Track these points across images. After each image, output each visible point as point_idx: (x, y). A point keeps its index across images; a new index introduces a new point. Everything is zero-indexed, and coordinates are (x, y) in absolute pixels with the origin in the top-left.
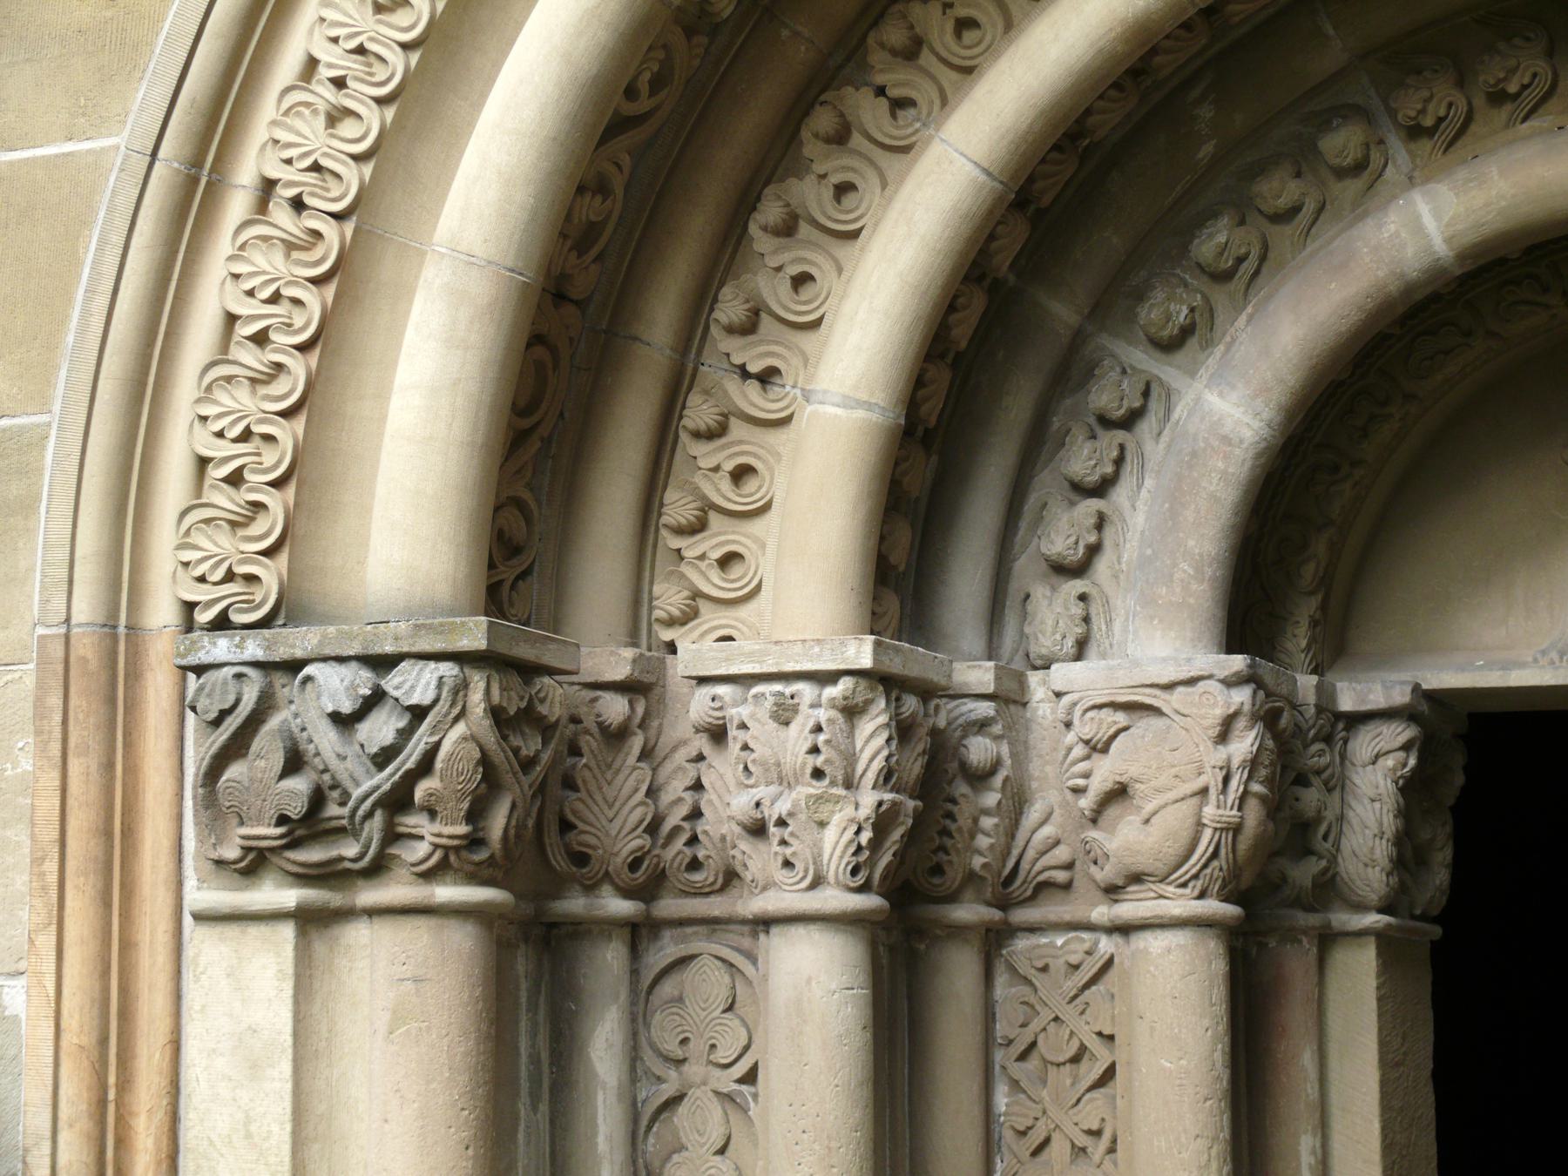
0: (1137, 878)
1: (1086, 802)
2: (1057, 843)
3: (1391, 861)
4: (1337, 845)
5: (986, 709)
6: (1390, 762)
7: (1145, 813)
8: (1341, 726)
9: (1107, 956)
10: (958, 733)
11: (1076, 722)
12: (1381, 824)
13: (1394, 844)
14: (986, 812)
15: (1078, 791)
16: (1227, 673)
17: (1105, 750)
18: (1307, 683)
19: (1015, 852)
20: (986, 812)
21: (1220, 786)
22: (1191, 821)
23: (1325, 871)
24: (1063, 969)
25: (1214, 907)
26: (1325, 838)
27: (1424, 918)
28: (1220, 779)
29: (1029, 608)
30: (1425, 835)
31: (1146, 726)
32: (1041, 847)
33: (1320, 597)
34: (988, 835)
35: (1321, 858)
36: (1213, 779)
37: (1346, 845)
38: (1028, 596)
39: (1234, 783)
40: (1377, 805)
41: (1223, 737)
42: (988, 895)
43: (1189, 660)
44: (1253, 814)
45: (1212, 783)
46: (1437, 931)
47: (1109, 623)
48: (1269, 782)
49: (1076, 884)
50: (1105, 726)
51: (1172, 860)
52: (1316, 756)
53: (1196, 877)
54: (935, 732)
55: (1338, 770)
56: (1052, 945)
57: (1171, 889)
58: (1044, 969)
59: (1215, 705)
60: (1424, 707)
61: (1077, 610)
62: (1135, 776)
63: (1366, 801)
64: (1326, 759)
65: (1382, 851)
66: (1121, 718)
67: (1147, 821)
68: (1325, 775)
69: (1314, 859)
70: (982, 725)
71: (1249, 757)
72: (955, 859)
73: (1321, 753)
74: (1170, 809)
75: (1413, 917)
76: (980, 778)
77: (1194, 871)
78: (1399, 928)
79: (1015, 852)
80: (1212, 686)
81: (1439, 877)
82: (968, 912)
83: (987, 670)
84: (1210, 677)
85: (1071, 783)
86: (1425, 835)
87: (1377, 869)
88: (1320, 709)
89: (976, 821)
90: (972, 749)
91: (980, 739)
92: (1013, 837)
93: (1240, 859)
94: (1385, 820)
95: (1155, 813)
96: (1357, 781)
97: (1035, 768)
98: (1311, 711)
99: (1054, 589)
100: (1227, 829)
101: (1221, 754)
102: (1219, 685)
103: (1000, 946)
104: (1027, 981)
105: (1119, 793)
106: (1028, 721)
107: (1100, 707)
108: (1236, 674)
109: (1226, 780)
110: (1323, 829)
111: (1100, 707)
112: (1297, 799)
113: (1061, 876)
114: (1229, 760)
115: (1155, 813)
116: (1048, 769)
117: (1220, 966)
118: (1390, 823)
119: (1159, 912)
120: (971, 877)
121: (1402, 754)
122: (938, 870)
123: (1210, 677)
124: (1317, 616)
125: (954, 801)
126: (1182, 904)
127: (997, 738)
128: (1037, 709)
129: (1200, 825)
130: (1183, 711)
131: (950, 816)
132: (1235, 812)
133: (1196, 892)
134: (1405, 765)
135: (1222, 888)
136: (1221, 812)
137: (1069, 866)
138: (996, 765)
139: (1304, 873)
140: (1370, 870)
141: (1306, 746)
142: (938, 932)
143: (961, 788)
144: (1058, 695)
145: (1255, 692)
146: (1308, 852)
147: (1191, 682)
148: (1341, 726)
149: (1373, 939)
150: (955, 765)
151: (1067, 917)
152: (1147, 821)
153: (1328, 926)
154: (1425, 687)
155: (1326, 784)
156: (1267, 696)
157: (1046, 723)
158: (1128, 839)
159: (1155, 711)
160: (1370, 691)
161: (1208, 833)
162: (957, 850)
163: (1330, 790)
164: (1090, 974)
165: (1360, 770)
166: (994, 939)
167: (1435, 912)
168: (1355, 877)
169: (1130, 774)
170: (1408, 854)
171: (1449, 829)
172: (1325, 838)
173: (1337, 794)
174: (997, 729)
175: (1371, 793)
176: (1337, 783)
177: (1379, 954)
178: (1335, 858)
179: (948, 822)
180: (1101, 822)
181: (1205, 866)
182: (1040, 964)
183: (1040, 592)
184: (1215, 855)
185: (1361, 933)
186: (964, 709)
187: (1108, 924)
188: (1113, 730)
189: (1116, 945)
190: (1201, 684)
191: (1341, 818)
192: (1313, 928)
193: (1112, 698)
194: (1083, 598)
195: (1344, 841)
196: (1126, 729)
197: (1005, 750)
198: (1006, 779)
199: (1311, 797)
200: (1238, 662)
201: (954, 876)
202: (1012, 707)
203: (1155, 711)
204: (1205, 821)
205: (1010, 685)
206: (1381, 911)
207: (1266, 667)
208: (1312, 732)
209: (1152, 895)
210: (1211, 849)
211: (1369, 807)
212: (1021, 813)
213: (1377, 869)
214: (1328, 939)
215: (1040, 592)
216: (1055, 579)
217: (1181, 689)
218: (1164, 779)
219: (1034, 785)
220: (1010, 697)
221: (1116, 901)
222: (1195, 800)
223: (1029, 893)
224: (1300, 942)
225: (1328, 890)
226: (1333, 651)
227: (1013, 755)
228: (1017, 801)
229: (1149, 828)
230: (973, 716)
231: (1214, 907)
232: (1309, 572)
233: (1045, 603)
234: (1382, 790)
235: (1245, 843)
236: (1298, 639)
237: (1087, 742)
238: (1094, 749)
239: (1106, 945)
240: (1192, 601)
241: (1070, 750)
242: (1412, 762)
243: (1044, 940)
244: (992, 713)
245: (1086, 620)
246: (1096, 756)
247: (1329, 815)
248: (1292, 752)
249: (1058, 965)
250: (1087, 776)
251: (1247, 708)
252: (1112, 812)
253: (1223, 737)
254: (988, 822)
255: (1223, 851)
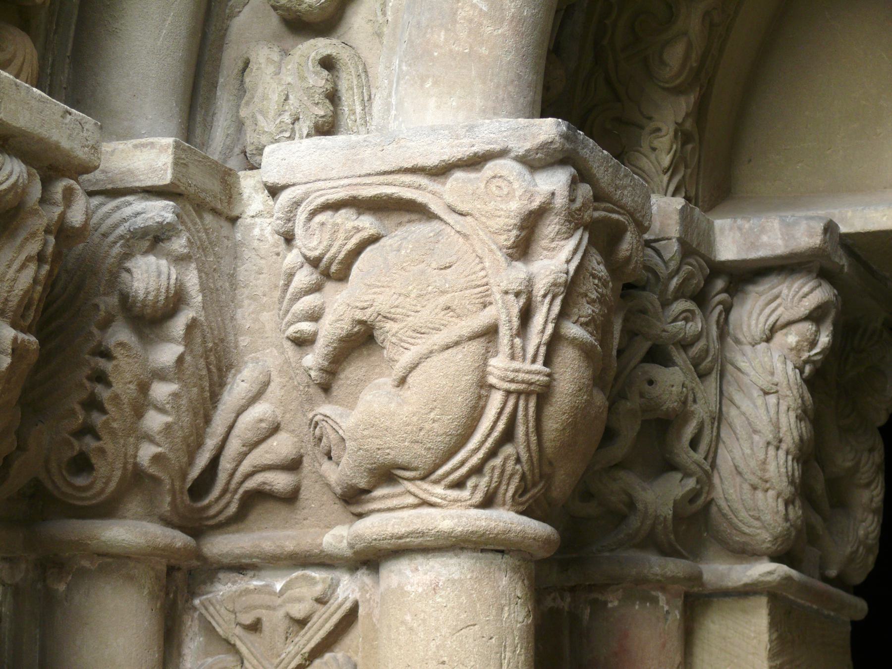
0: (387, 474)
1: (313, 359)
2: (275, 429)
3: (792, 482)
4: (712, 457)
5: (160, 211)
6: (791, 338)
7: (398, 370)
8: (720, 284)
9: (348, 605)
10: (117, 250)
11: (299, 231)
12: (777, 427)
13: (796, 459)
14: (160, 375)
15: (302, 342)
16: (528, 145)
17: (342, 276)
18: (666, 210)
19: (211, 444)
20: (160, 375)
21: (516, 322)
22: (468, 379)
23: (693, 497)
24: (283, 625)
25: (505, 519)
26: (694, 444)
27: (839, 582)
28: (515, 311)
29: (247, 80)
30: (844, 460)
31: (407, 235)
32: (251, 436)
33: (692, 98)
34: (162, 410)
35: (687, 474)
36: (505, 313)
37: (724, 458)
38: (247, 63)
39: (538, 320)
40: (772, 399)
41: (523, 248)
42: (165, 505)
43: (471, 128)
44: (570, 372)
45: (503, 317)
46: (860, 607)
47: (367, 102)
48: (599, 326)
49: (303, 494)
50: (341, 235)
51: (440, 443)
52: (679, 320)
53: (477, 470)
54: (64, 233)
55: (714, 345)
56: (267, 590)
57: (439, 490)
58: (255, 627)
59: (509, 196)
60: (842, 260)
61: (319, 80)
62: (384, 309)
63: (756, 393)
64: (695, 326)
65: (779, 467)
66: (368, 224)
67: (402, 381)
68: (695, 350)
69: (679, 476)
70: (155, 238)
71: (563, 278)
72: (109, 447)
73: (688, 316)
74: (436, 359)
75: (825, 579)
76: (150, 320)
77: (474, 460)
78: (804, 589)
79: (211, 444)
80: (507, 167)
81: (864, 526)
82: (126, 532)
83: (163, 149)
84: (503, 153)
85: (291, 330)
86: (844, 460)
87: (771, 493)
88: (687, 250)
89: (144, 388)
90: (137, 273)
91: (152, 259)
92: (208, 420)
93: (548, 444)
94: (783, 420)
95: (414, 367)
96: (743, 364)
97: (246, 315)
98: (675, 247)
99: (285, 53)
100: (528, 394)
101: (517, 274)
102: (518, 167)
103: (193, 594)
104: (232, 648)
105: (361, 340)
106: (236, 245)
107: (335, 206)
108: (544, 146)
109: (526, 315)
110: (689, 431)
111: (335, 206)
112: (651, 382)
113: (280, 481)
114: (530, 282)
115: (414, 367)
116: (265, 316)
117: (516, 617)
118: (791, 428)
119: (418, 526)
120: (137, 479)
121: (808, 327)
122: (82, 464)
123: (503, 153)
124: (689, 125)
125: (107, 355)
126: (456, 515)
127: (180, 260)
128: (251, 227)
129: (484, 387)
130: (461, 207)
131: (101, 378)
132: (539, 366)
133: (479, 497)
134: (813, 344)
135: (522, 491)
136: (516, 365)
137: (293, 465)
138: (176, 300)
139: (662, 496)
140: (760, 494)
141: (666, 304)
142: (86, 563)
143: (121, 335)
144: (274, 191)
145: (573, 183)
146: (670, 466)
147: (475, 162)
148: (720, 284)
149: (764, 600)
150: (113, 300)
151: (290, 546)
152: (402, 381)
153: (696, 578)
154: (843, 229)
155: (696, 366)
156: (599, 197)
157: (264, 247)
158: (379, 411)
159: (415, 210)
160: (763, 230)
161: (496, 400)
162: (113, 433)
163: (703, 376)
164: (322, 633)
165: (748, 349)
166: (178, 584)
167: (858, 578)
168: (737, 506)
169: (377, 307)
170: (816, 481)
171: (878, 457)
172: (694, 444)
173: (712, 382)
174: (179, 244)
175: (764, 381)
176: (712, 367)
177: (774, 624)
178: (709, 477)
179: (99, 388)
180: (336, 391)
181: (492, 453)
182: (248, 619)
183: (263, 57)
184: (508, 436)
185: (747, 592)
186: (127, 211)
187: (349, 553)
188: (351, 244)
189: (362, 589)
190: (490, 165)
191: (719, 418)
192: (674, 580)
193: (354, 192)
194: (328, 64)
195: (722, 452)
196: (373, 240)
197: (192, 279)
198: (192, 326)
199: (672, 381)
200: (549, 129)
201: (107, 475)
202: (209, 218)
203: (415, 210)
204: (492, 380)
205: (202, 182)
206: (774, 558)
207: (595, 154)
208: (675, 282)
209: (411, 500)
210: (501, 426)
211: (760, 401)
212: (222, 385)
213: (771, 493)
214: (697, 602)
215: (263, 57)
216: (290, 40)
217: (459, 175)
218: (427, 315)
219: (244, 341)
220: (205, 199)
221: (360, 516)
222: (476, 347)
223: (233, 508)
224: (655, 601)
225: (697, 525)
226: (716, 181)
227: (203, 288)
228: (213, 365)
229: (406, 393)
230: (140, 222)
231: (505, 519)
232: (675, 55)
233: (271, 69)
234: (779, 377)
235: (554, 421)
236: (661, 150)
237: (314, 263)
238: (327, 275)
239: (349, 588)
240: (484, 51)
241: (291, 276)
242: (824, 339)
243: (256, 583)
244: (169, 217)
245: (333, 97)
246: (330, 286)
247: (701, 411)
248: (644, 311)
249: (274, 620)
250: (315, 316)
251: (560, 201)
252: (352, 372)
253: (523, 248)
254: (161, 391)
255: (520, 431)
